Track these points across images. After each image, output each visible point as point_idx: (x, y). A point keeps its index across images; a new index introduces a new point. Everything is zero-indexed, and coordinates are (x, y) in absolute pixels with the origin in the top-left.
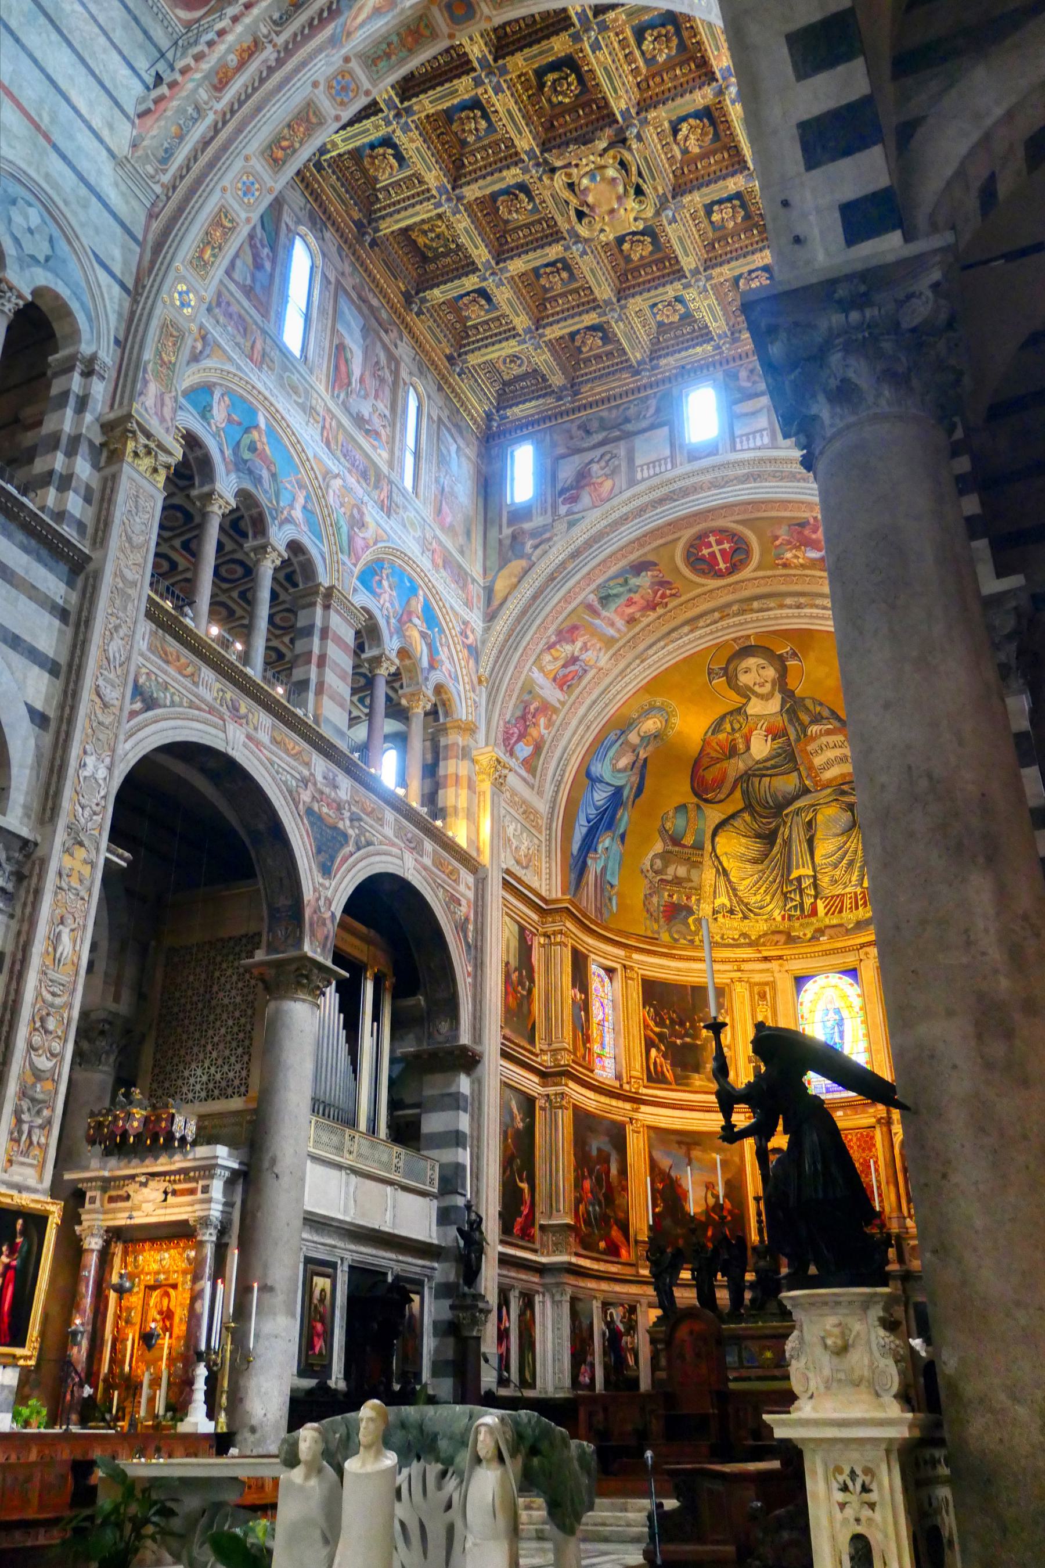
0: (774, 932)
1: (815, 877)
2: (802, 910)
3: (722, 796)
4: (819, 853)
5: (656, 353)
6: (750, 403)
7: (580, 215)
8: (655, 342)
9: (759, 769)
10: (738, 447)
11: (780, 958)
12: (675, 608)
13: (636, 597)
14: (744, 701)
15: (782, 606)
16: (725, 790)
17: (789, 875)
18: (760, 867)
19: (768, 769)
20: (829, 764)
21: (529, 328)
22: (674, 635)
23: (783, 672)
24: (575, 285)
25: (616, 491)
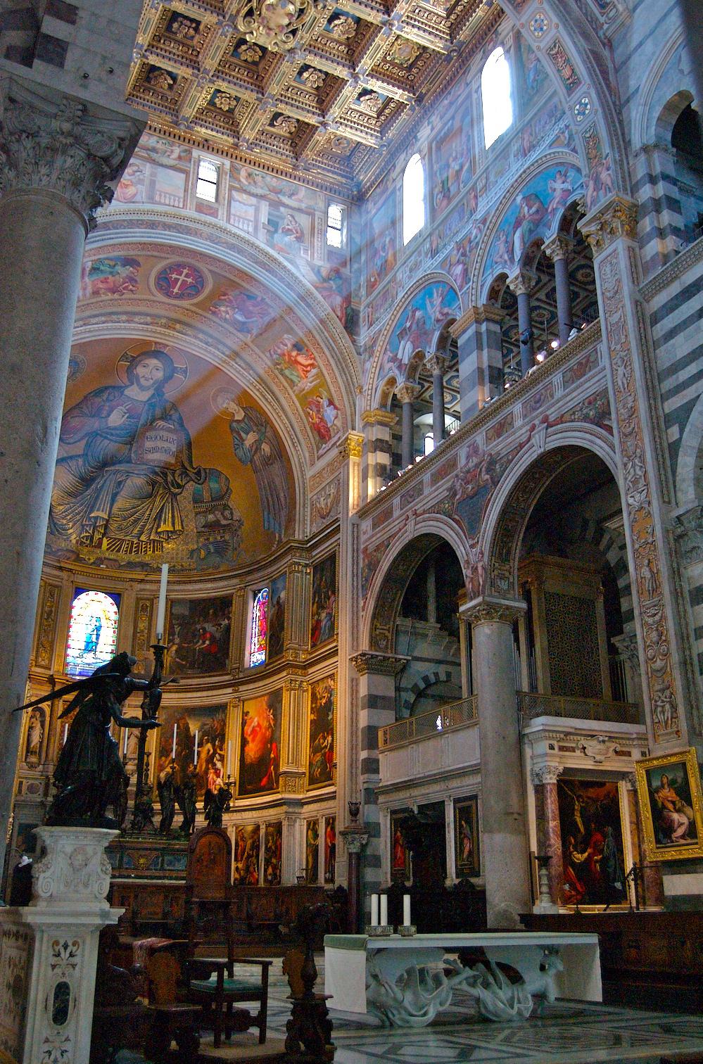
0: (67, 550)
1: (108, 521)
2: (92, 541)
3: (72, 441)
4: (116, 506)
5: (197, 120)
6: (245, 196)
7: (250, 13)
8: (201, 111)
9: (107, 433)
10: (232, 221)
11: (71, 570)
12: (125, 299)
13: (111, 278)
14: (128, 383)
15: (196, 337)
16: (76, 437)
17: (90, 513)
18: (74, 500)
19: (112, 435)
20: (155, 450)
21: (142, 46)
22: (114, 317)
23: (168, 378)
24: (189, 42)
25: (138, 198)
